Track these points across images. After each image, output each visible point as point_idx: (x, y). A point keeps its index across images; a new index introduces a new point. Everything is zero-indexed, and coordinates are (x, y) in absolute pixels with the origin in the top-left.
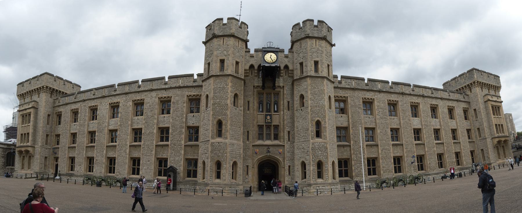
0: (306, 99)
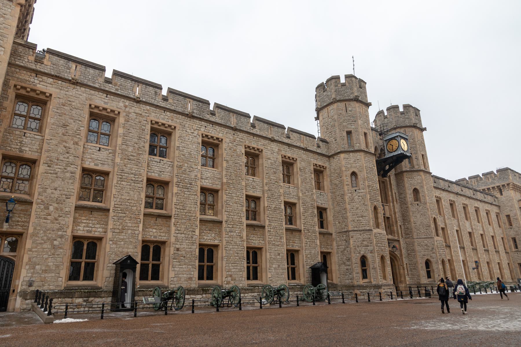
0: (423, 194)
